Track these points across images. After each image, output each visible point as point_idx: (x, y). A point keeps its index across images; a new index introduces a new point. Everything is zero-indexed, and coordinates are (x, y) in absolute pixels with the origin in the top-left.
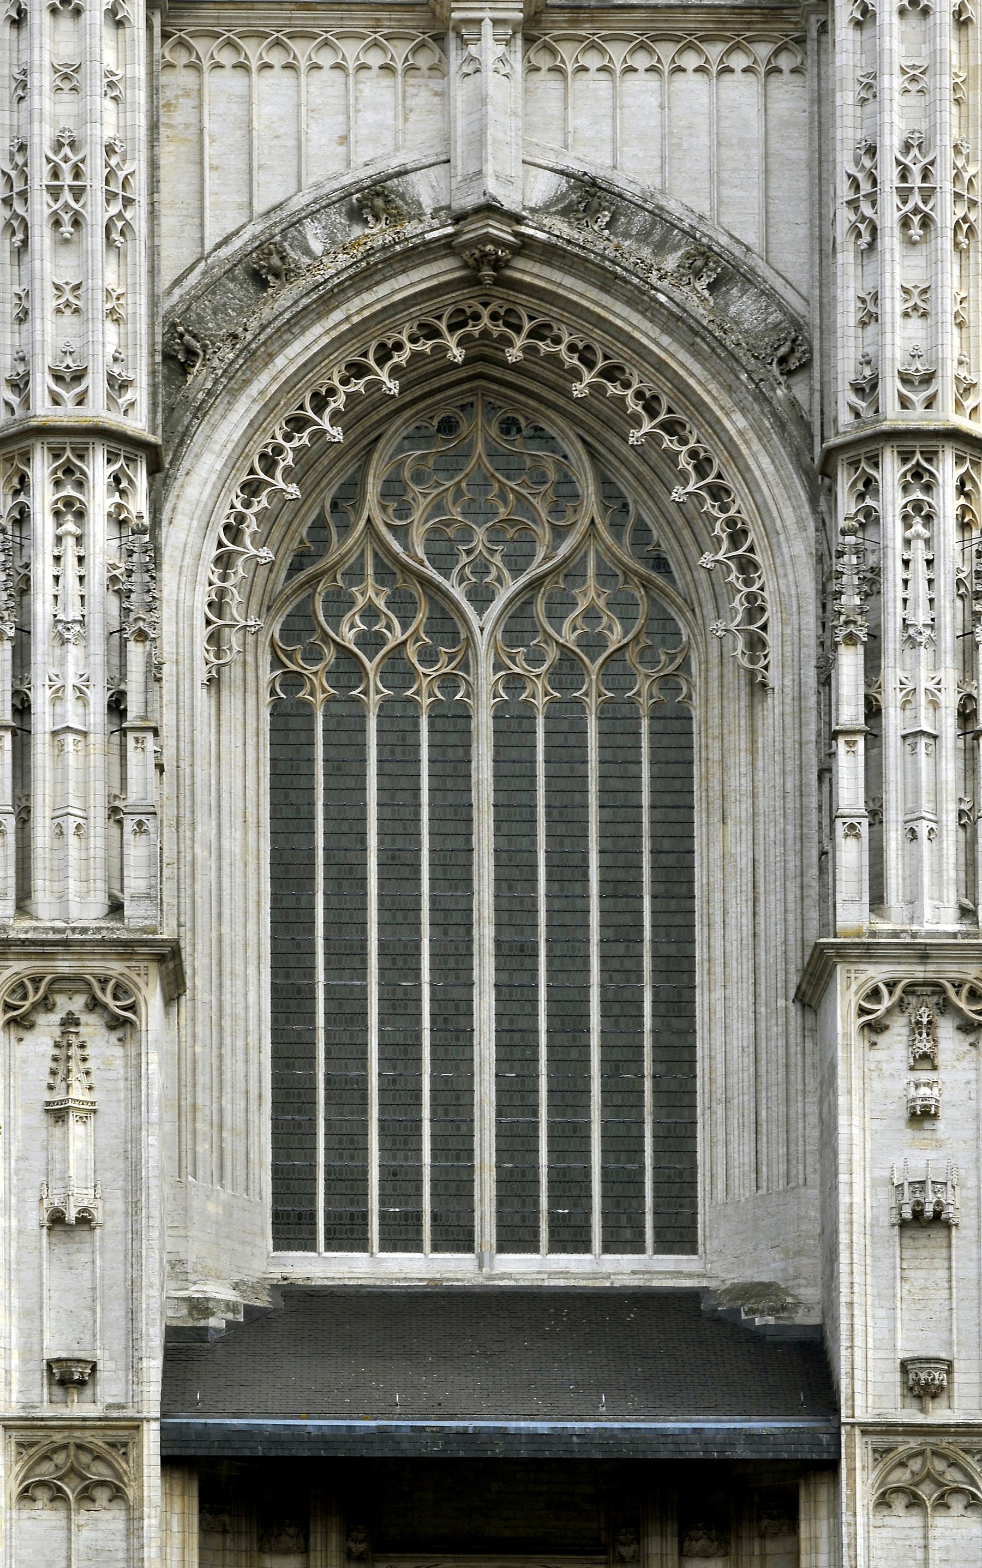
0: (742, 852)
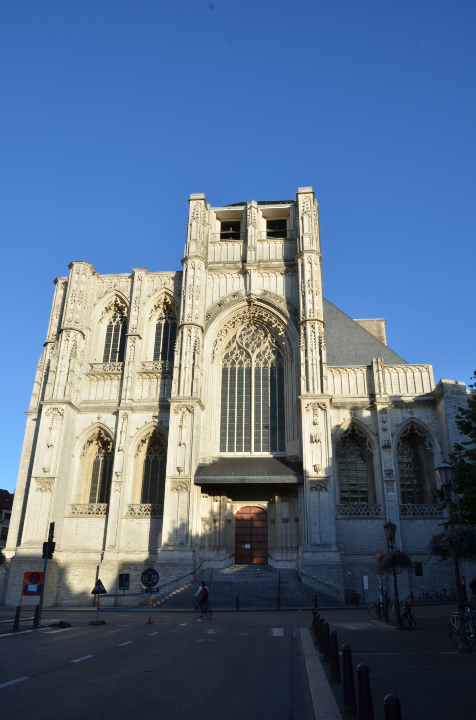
0: (290, 387)
